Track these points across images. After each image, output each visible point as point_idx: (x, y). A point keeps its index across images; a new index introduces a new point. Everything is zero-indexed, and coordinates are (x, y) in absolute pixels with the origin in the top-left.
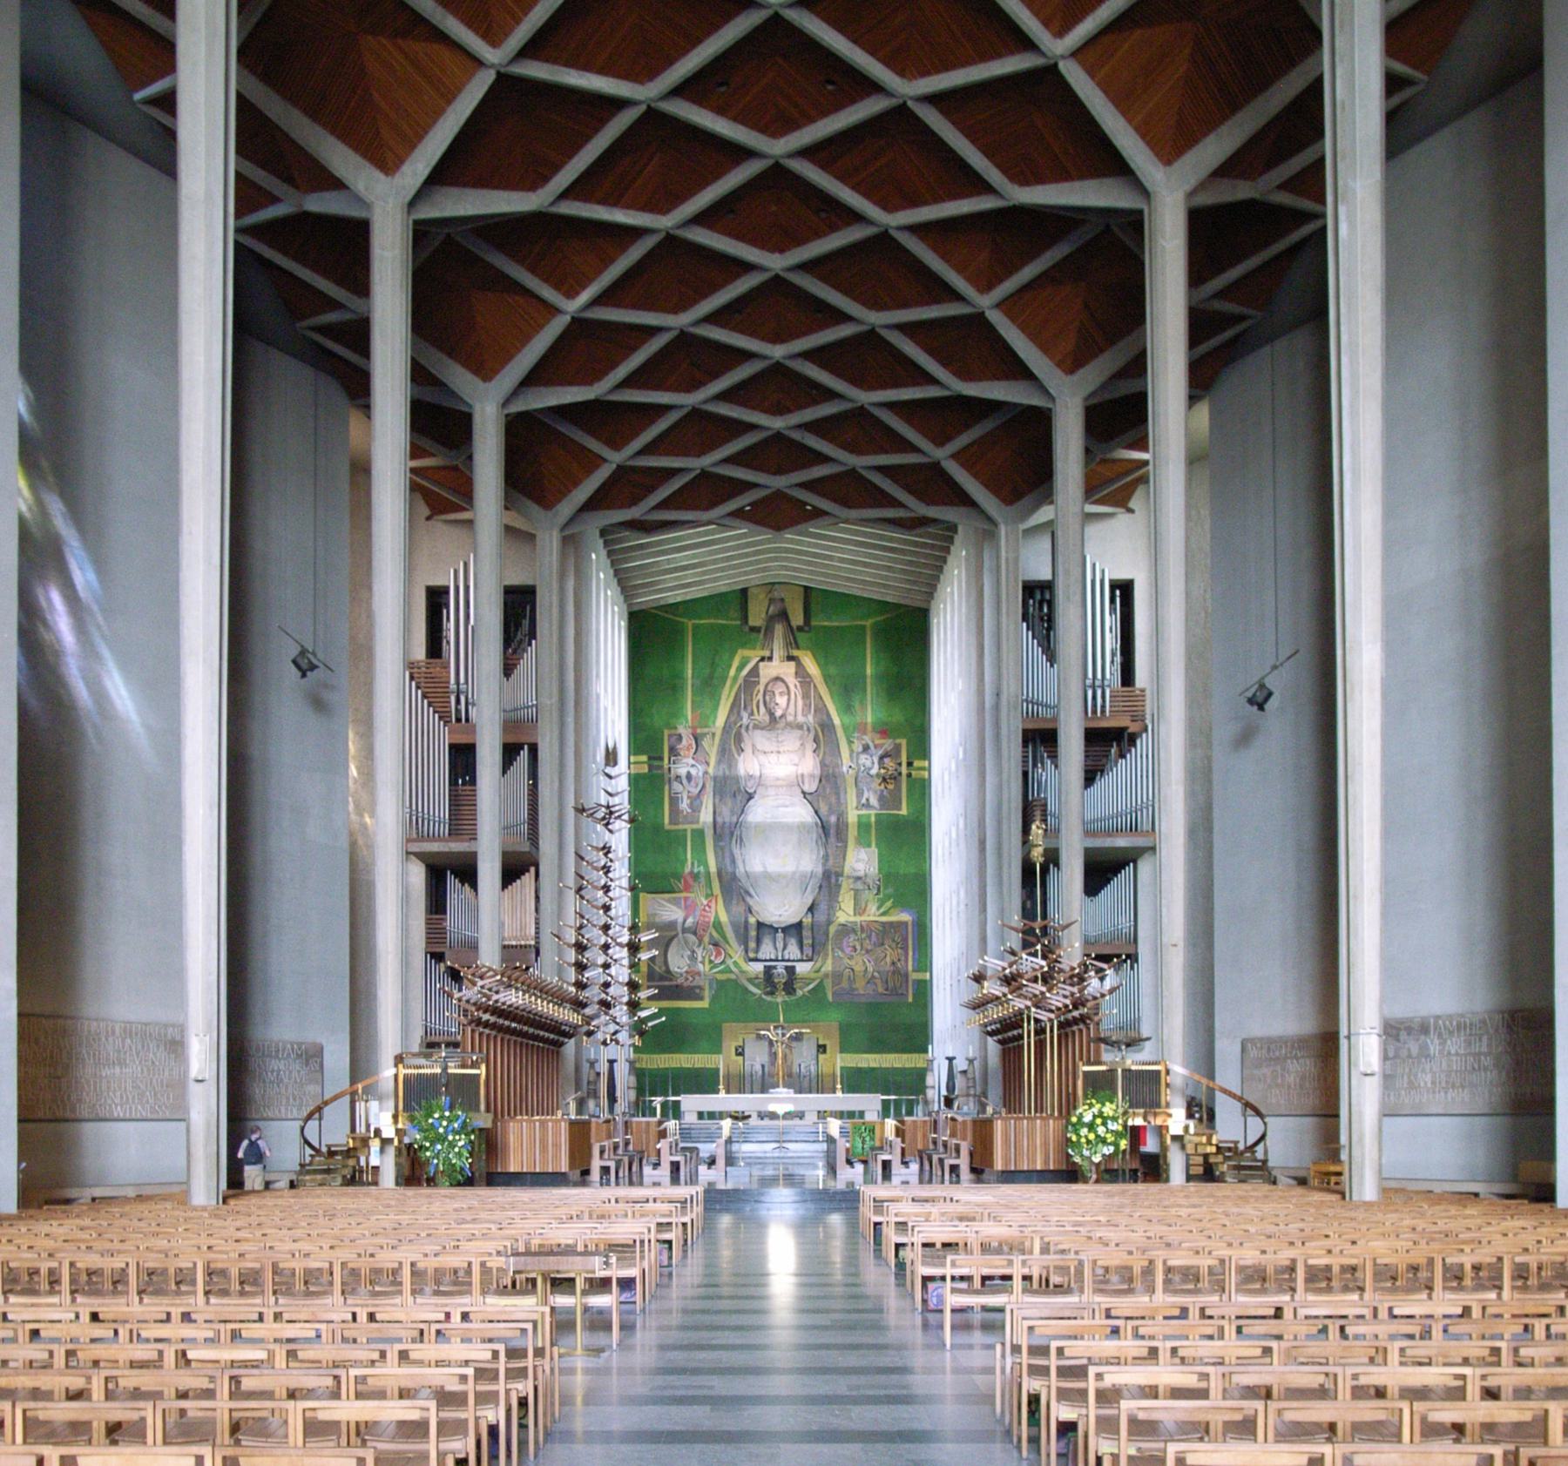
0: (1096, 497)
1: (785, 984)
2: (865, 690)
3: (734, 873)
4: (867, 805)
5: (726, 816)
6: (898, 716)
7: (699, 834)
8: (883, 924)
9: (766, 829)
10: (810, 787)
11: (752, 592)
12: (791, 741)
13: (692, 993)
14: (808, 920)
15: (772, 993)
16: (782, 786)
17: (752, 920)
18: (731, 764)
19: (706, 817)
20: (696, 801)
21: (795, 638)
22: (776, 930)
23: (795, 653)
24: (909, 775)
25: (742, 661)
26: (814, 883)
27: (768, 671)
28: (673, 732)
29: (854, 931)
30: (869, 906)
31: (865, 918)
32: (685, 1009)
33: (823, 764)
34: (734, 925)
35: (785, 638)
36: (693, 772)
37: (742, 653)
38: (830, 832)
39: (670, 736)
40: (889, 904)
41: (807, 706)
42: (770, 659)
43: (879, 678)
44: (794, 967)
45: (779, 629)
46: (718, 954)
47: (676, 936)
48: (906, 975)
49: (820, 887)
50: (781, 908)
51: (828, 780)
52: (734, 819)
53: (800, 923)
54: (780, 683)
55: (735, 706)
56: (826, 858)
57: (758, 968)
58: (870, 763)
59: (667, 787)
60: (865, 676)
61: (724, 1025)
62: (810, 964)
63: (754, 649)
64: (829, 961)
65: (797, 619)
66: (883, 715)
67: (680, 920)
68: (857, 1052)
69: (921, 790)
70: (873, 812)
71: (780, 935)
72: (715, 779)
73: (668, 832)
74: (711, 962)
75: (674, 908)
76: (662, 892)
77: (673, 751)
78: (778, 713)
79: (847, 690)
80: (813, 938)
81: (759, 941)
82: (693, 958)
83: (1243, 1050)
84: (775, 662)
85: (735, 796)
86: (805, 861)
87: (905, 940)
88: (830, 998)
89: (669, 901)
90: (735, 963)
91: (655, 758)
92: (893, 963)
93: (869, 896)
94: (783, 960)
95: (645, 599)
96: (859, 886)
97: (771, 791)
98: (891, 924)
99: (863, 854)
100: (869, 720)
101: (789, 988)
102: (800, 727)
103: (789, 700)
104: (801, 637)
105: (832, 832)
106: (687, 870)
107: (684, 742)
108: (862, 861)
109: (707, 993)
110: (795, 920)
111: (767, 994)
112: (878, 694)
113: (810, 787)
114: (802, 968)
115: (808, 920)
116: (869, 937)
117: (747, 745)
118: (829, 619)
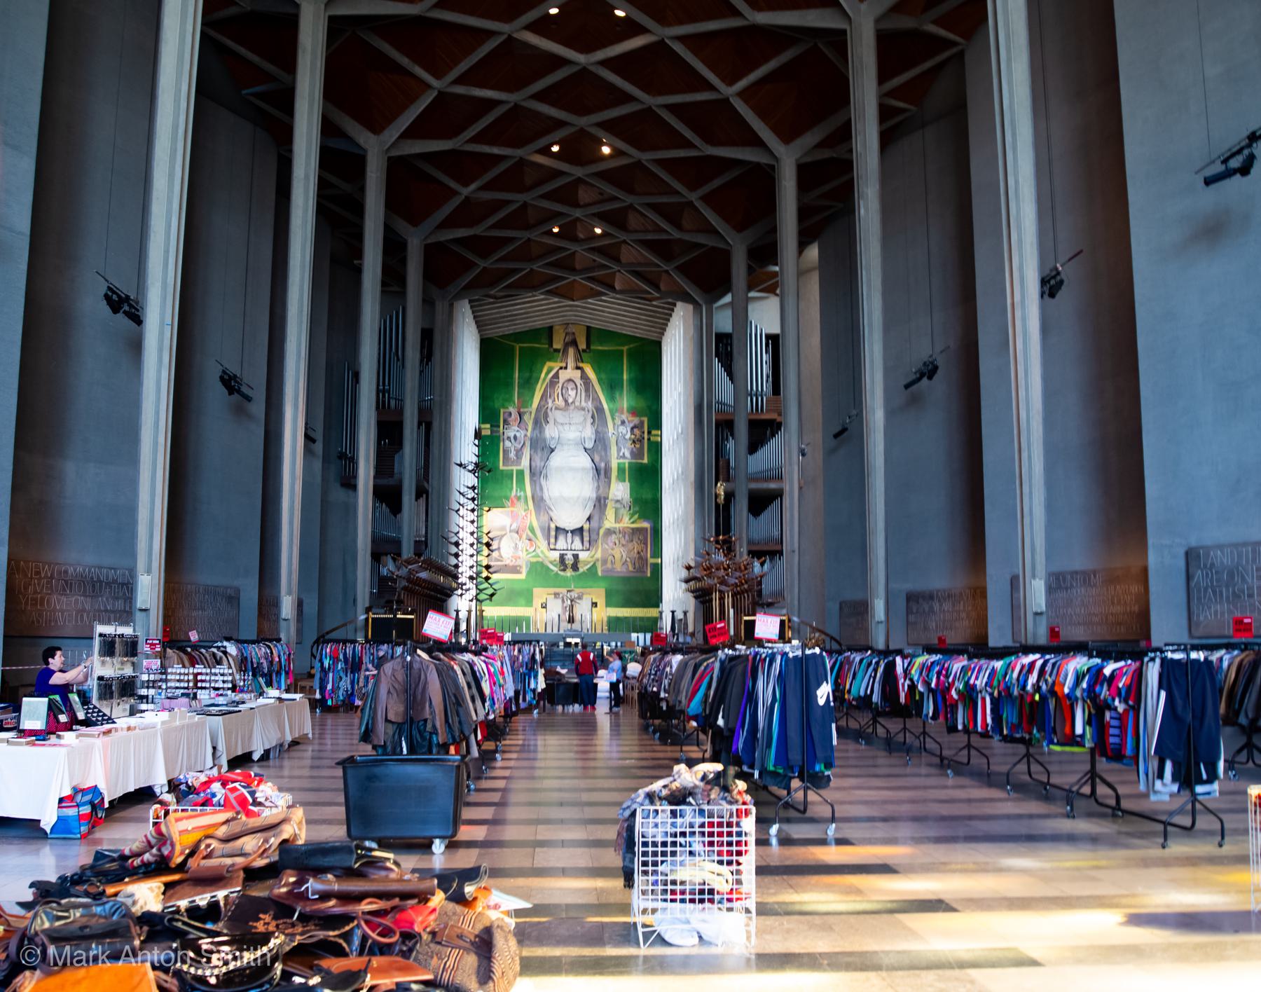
0: (760, 288)
1: (572, 565)
2: (622, 387)
4: (624, 457)
6: (641, 404)
7: (521, 474)
8: (633, 529)
10: (589, 445)
11: (556, 328)
12: (577, 417)
14: (586, 527)
15: (564, 570)
17: (553, 526)
18: (541, 430)
19: (525, 462)
20: (519, 453)
22: (567, 532)
23: (581, 365)
24: (649, 439)
25: (548, 369)
27: (564, 375)
28: (507, 410)
29: (615, 533)
33: (597, 432)
34: (542, 529)
36: (518, 435)
37: (548, 364)
38: (601, 473)
39: (504, 413)
40: (636, 516)
41: (588, 396)
42: (566, 368)
43: (630, 381)
45: (571, 351)
46: (532, 545)
49: (595, 506)
50: (572, 518)
51: (600, 440)
52: (542, 464)
54: (571, 383)
56: (598, 488)
57: (556, 555)
58: (625, 431)
59: (501, 444)
60: (622, 380)
61: (534, 589)
63: (556, 361)
65: (582, 346)
66: (633, 403)
69: (656, 449)
71: (569, 535)
73: (502, 471)
74: (527, 550)
77: (505, 422)
79: (612, 387)
81: (556, 538)
82: (516, 547)
83: (841, 608)
86: (586, 488)
88: (600, 574)
89: (502, 512)
90: (542, 552)
91: (495, 425)
92: (638, 553)
95: (494, 332)
96: (618, 505)
97: (566, 447)
100: (625, 406)
101: (575, 567)
102: (583, 409)
104: (583, 355)
105: (602, 472)
106: (513, 493)
108: (620, 490)
110: (579, 526)
112: (630, 390)
113: (589, 445)
114: (583, 556)
117: (551, 419)
118: (601, 345)
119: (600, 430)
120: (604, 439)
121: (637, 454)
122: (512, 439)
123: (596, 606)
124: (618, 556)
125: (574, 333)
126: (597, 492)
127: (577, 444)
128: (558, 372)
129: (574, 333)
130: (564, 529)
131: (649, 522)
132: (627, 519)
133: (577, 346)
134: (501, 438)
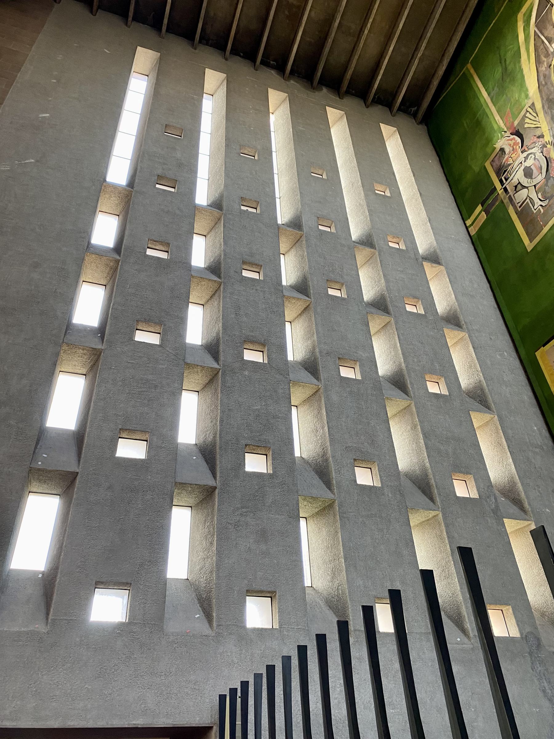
36: (529, 163)
107: (507, 151)
134: (506, 201)
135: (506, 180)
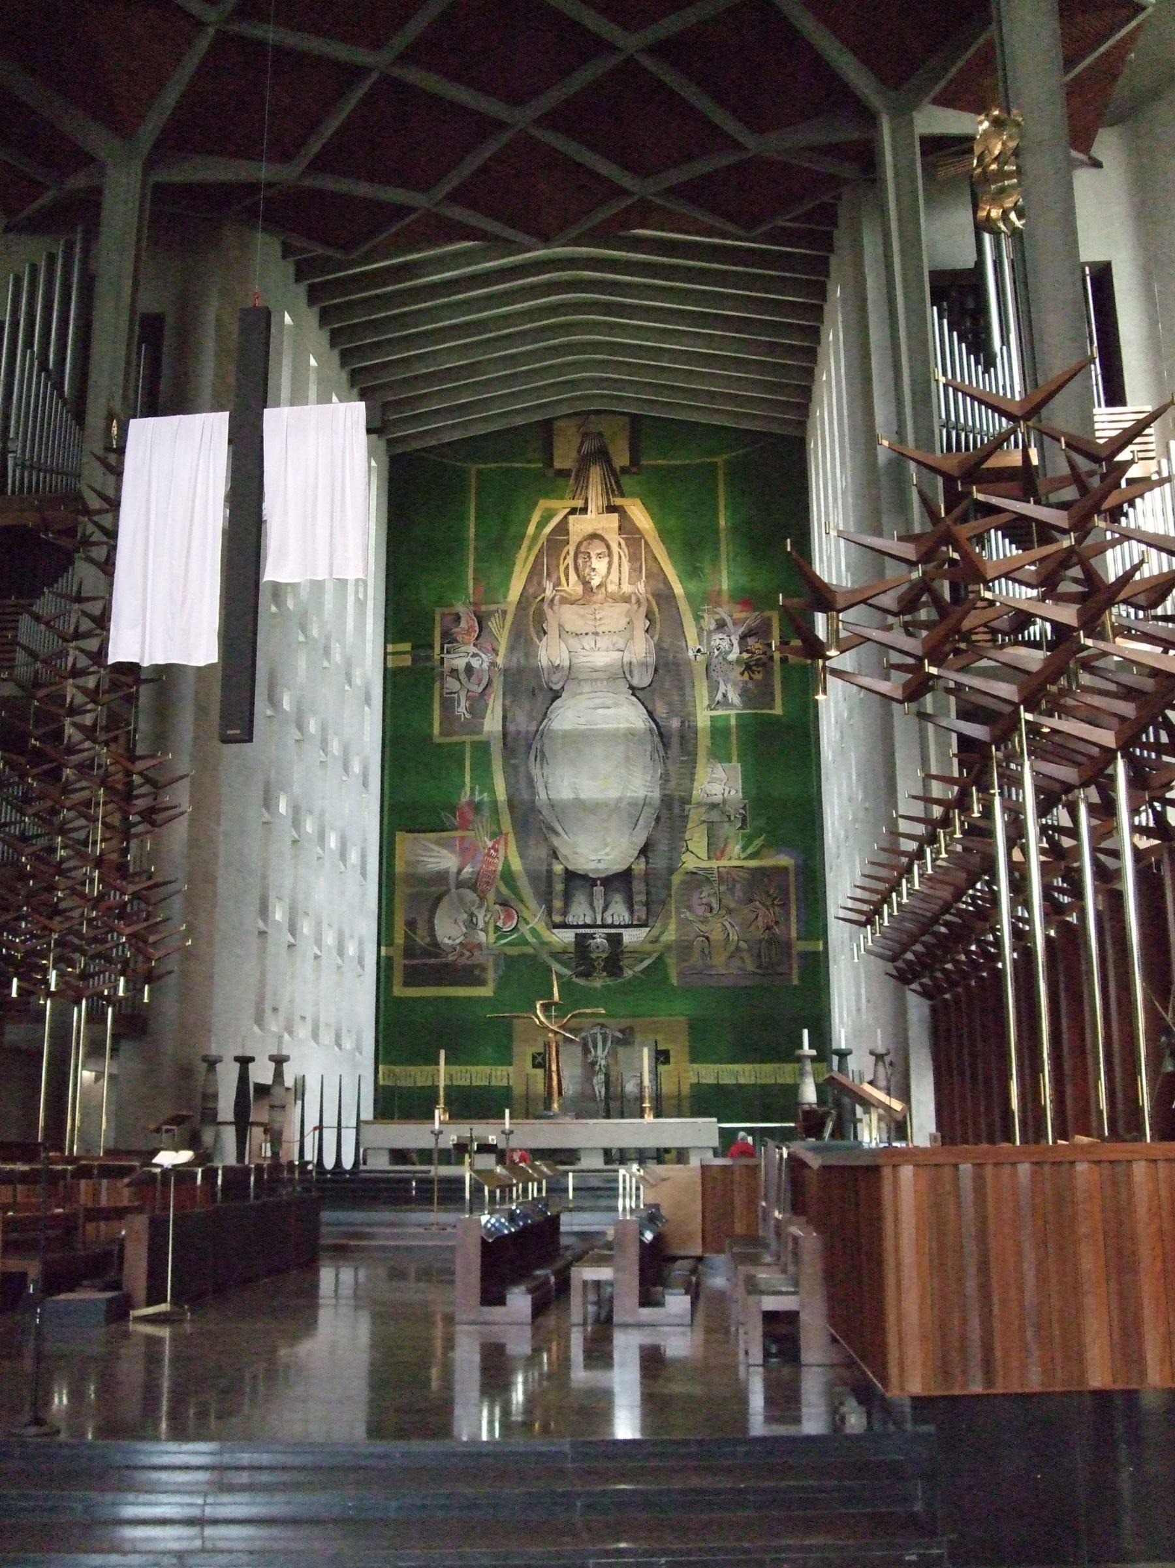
3: (533, 802)
4: (725, 703)
5: (522, 722)
7: (482, 749)
8: (754, 871)
9: (580, 740)
13: (470, 975)
14: (640, 867)
15: (586, 975)
16: (602, 680)
17: (558, 868)
18: (530, 651)
19: (492, 724)
20: (478, 706)
21: (617, 482)
22: (593, 882)
23: (618, 501)
24: (784, 660)
26: (648, 815)
27: (580, 526)
28: (446, 611)
30: (730, 847)
31: (724, 862)
32: (457, 998)
33: (659, 648)
34: (533, 878)
35: (604, 481)
36: (475, 663)
37: (544, 504)
39: (443, 616)
40: (759, 842)
41: (636, 571)
42: (584, 510)
43: (735, 530)
44: (620, 935)
45: (596, 474)
46: (509, 917)
47: (447, 892)
48: (788, 945)
49: (658, 819)
52: (533, 728)
53: (629, 870)
54: (597, 542)
55: (535, 573)
56: (665, 778)
58: (729, 646)
59: (437, 685)
60: (717, 531)
62: (641, 933)
63: (562, 498)
64: (672, 926)
65: (621, 459)
66: (743, 581)
67: (454, 869)
68: (720, 1061)
70: (733, 712)
71: (599, 890)
72: (506, 672)
73: (439, 745)
74: (497, 929)
75: (444, 852)
76: (424, 832)
77: (448, 637)
78: (595, 582)
80: (648, 894)
81: (567, 898)
82: (471, 924)
84: (591, 515)
85: (534, 695)
87: (785, 892)
88: (674, 981)
89: (438, 843)
90: (533, 930)
91: (422, 645)
92: (768, 928)
93: (729, 830)
94: (603, 926)
96: (715, 816)
97: (586, 688)
98: (761, 871)
99: (719, 771)
100: (725, 587)
103: (610, 564)
104: (625, 480)
105: (675, 741)
106: (465, 796)
107: (463, 624)
109: (491, 975)
110: (625, 867)
111: (580, 975)
113: (642, 679)
114: (631, 937)
115: (640, 867)
116: (731, 890)
117: (551, 626)
119: (665, 646)
120: (677, 665)
121: (758, 694)
122: (462, 676)
123: (667, 1061)
124: (717, 935)
125: (601, 435)
126: (663, 788)
127: (612, 678)
128: (565, 519)
129: (601, 435)
130: (584, 877)
131: (791, 856)
132: (738, 848)
133: (608, 461)
135: (448, 652)
